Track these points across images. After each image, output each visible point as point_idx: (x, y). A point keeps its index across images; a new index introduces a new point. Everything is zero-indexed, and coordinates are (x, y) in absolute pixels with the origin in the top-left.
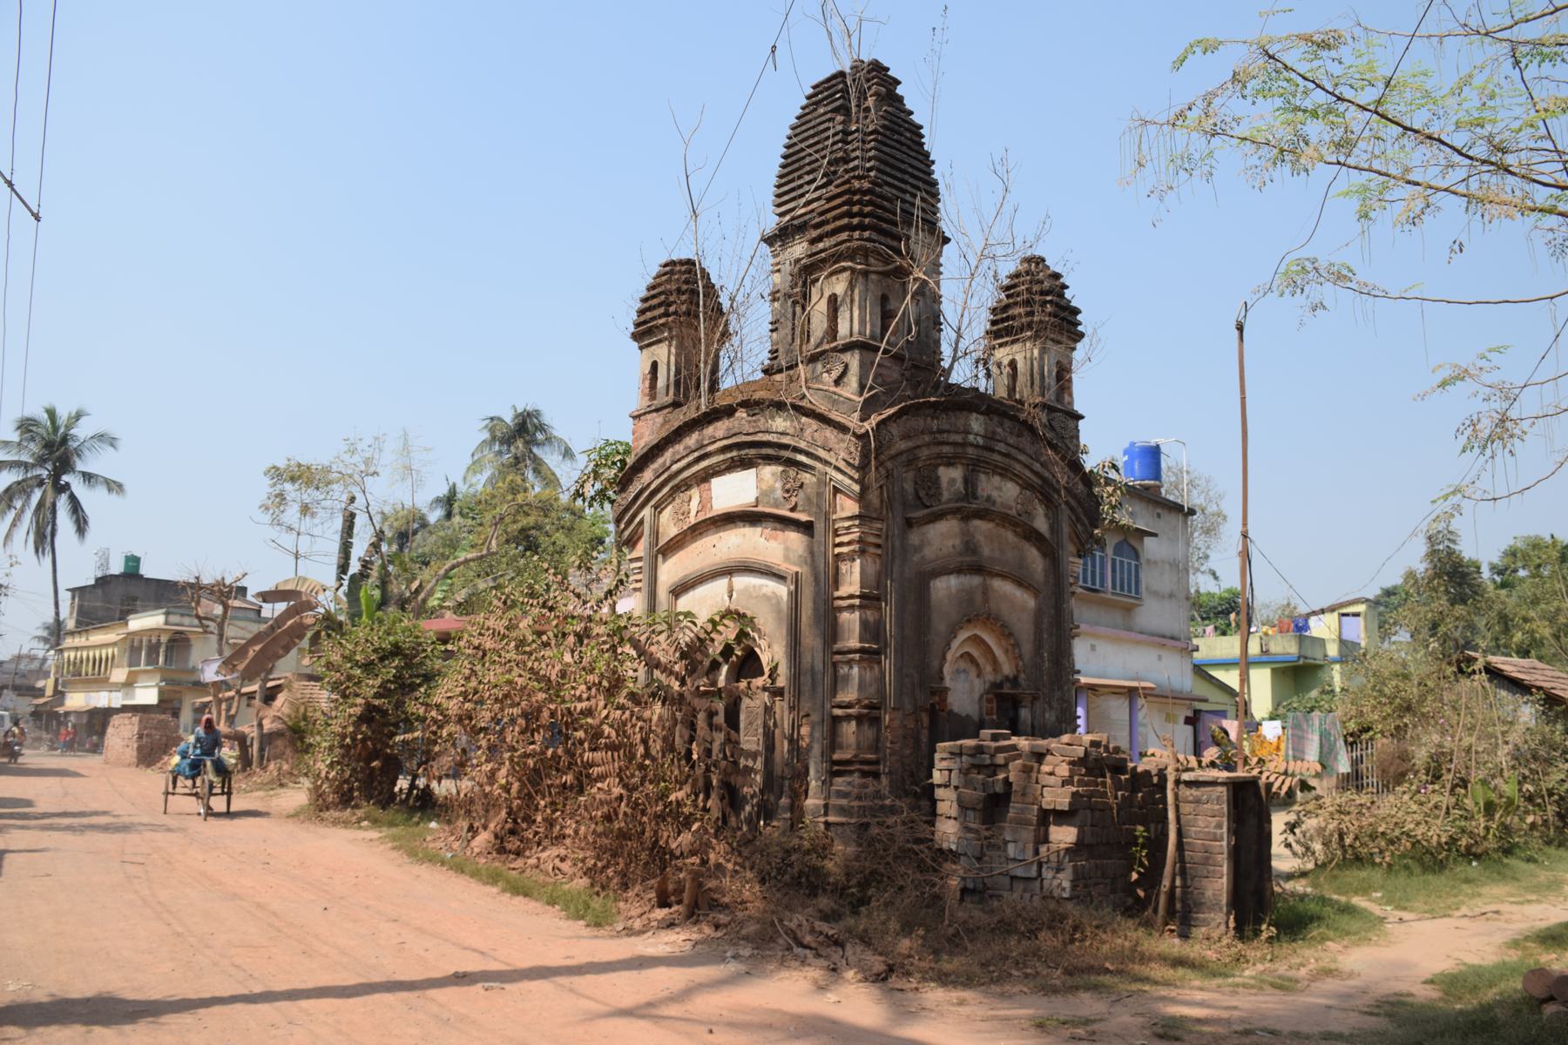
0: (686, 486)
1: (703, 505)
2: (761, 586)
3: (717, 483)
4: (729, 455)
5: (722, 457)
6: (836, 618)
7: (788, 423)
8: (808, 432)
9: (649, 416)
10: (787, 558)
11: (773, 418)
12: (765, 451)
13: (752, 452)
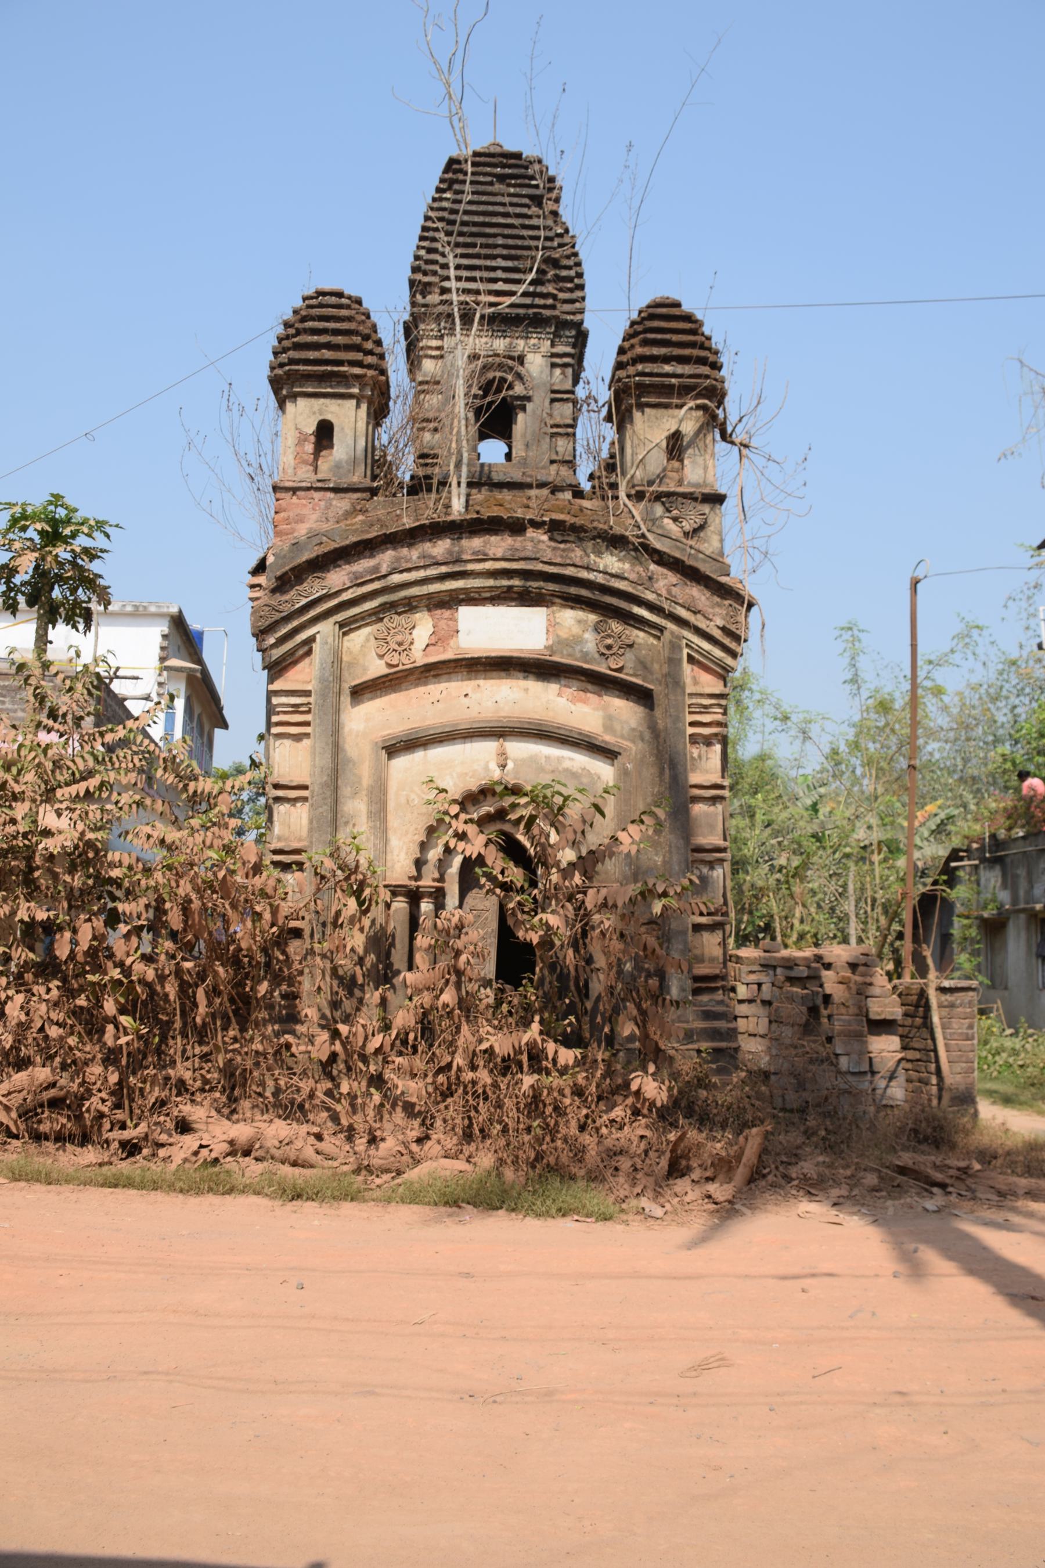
0: (410, 606)
1: (437, 640)
2: (560, 759)
3: (466, 614)
4: (505, 582)
5: (491, 582)
6: (687, 811)
7: (627, 566)
8: (661, 585)
9: (317, 495)
10: (608, 728)
11: (599, 554)
12: (573, 590)
13: (552, 587)
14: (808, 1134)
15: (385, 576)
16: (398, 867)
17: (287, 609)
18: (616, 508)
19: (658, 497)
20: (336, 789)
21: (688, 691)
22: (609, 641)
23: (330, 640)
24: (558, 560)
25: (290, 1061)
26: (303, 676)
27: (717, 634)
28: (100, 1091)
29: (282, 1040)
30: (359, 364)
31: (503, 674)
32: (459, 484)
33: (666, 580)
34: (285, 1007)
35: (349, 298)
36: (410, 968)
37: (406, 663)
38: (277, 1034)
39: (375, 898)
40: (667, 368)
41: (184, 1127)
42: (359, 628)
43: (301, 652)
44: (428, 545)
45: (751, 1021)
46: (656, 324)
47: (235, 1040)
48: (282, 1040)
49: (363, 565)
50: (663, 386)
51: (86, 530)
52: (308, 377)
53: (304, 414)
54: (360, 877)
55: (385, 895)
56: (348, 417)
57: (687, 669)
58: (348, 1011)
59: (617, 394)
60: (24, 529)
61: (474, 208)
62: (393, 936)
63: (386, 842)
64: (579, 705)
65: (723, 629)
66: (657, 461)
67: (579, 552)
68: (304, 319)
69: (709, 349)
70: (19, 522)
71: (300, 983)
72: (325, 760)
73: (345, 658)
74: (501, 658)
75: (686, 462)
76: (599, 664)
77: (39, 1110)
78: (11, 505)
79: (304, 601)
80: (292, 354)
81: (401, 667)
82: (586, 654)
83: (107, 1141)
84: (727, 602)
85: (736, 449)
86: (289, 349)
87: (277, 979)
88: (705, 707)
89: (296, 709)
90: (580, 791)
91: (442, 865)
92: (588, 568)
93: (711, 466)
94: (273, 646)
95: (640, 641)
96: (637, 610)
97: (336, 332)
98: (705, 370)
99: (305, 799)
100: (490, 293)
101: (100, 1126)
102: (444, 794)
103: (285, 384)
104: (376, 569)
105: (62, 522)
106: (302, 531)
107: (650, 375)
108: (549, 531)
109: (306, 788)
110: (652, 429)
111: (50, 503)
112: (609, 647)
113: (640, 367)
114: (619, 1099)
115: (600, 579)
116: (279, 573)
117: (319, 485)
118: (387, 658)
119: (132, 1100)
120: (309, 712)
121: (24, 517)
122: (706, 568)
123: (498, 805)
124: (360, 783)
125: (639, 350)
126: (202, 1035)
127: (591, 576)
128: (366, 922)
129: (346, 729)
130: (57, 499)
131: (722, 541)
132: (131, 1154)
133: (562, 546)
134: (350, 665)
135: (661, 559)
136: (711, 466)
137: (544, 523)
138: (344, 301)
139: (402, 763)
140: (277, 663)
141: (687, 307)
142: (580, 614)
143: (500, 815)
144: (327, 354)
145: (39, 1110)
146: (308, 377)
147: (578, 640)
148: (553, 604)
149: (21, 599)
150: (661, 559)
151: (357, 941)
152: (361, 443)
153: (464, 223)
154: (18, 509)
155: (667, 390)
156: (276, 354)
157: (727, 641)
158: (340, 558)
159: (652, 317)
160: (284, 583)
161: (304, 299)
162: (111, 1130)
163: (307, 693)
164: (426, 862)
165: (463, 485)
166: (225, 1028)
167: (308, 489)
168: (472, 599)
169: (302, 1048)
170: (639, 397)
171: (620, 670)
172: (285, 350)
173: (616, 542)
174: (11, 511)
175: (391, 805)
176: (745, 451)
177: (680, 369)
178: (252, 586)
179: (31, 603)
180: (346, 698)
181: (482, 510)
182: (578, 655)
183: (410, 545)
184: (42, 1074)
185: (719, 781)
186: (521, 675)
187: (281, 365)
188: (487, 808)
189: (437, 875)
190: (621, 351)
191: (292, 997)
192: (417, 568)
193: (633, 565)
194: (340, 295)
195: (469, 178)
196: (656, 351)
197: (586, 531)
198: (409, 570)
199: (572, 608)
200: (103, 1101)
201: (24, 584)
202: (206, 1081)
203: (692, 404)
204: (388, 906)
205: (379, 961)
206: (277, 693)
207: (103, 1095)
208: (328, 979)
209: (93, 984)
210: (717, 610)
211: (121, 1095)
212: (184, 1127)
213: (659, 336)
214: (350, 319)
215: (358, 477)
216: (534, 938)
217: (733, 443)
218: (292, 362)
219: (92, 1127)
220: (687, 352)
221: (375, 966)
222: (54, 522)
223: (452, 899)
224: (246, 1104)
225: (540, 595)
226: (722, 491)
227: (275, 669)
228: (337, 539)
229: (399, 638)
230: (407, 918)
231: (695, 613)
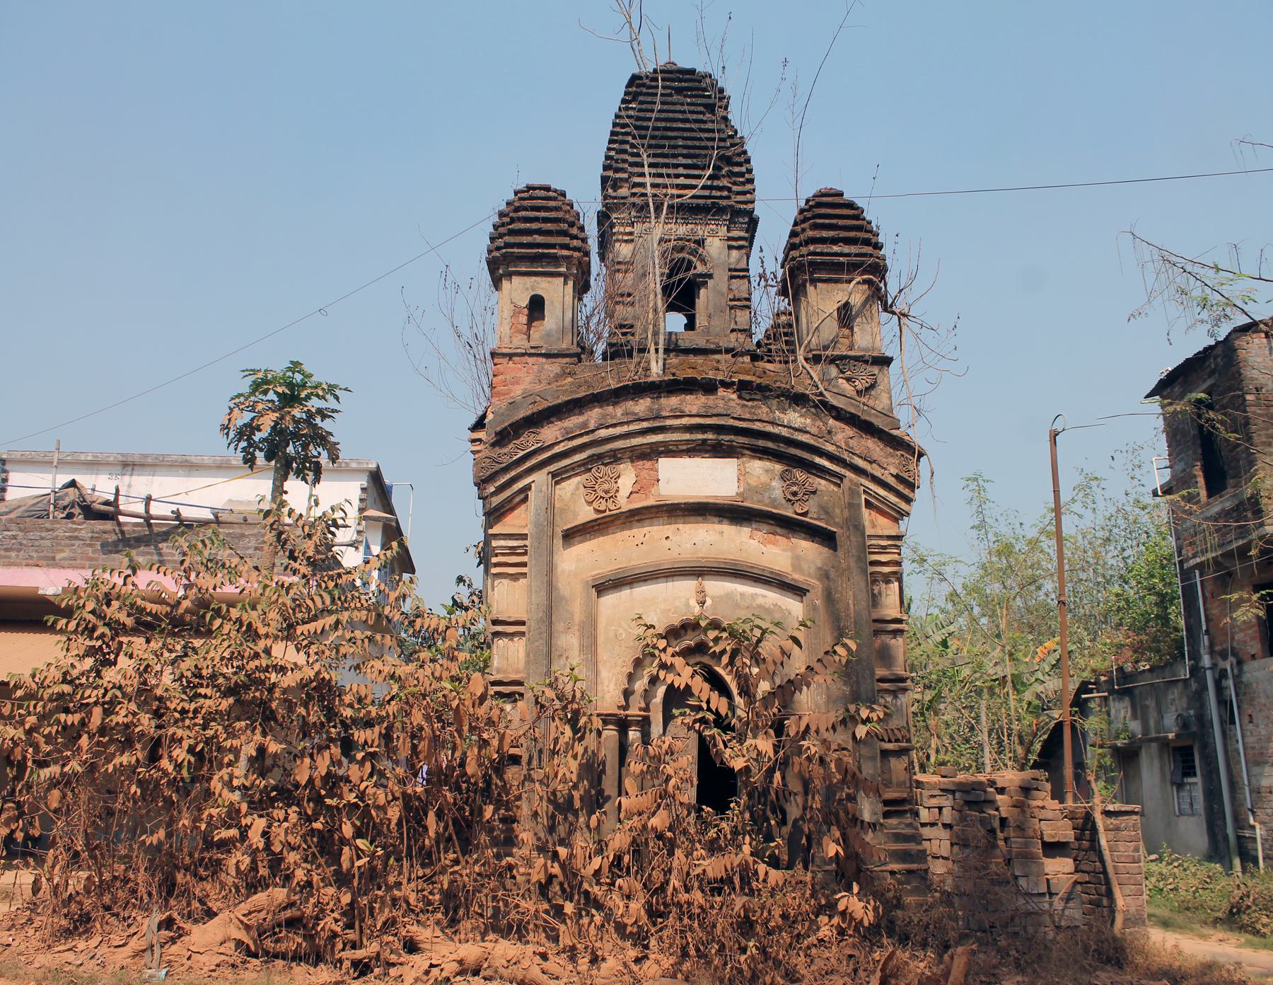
0: (615, 457)
2: (754, 596)
3: (664, 464)
4: (700, 436)
5: (687, 436)
7: (808, 421)
10: (796, 567)
11: (783, 411)
12: (761, 443)
13: (741, 440)
14: (1003, 953)
15: (593, 431)
16: (607, 696)
17: (506, 461)
18: (796, 369)
19: (832, 360)
20: (551, 624)
21: (867, 533)
22: (795, 489)
23: (544, 488)
24: (747, 416)
25: (509, 883)
26: (516, 521)
27: (892, 481)
28: (332, 911)
29: (504, 863)
30: (566, 247)
31: (700, 518)
32: (657, 350)
33: (843, 434)
34: (502, 832)
35: (555, 191)
36: (620, 795)
37: (611, 508)
38: (498, 857)
39: (589, 726)
40: (836, 249)
41: (412, 947)
42: (569, 477)
43: (517, 499)
44: (629, 405)
45: (938, 842)
46: (823, 211)
47: (456, 862)
48: (504, 863)
49: (573, 422)
50: (833, 264)
51: (321, 393)
52: (522, 258)
53: (519, 289)
54: (575, 706)
55: (597, 723)
56: (556, 292)
57: (865, 512)
58: (563, 835)
59: (791, 270)
60: (265, 392)
61: (664, 115)
62: (604, 763)
63: (597, 674)
64: (769, 546)
65: (897, 477)
66: (830, 329)
67: (765, 409)
68: (517, 210)
69: (871, 232)
70: (260, 386)
71: (518, 807)
72: (541, 598)
73: (557, 505)
74: (699, 503)
75: (855, 329)
76: (786, 509)
77: (277, 930)
78: (255, 372)
79: (521, 454)
80: (508, 239)
81: (608, 513)
82: (774, 500)
83: (341, 961)
84: (899, 453)
85: (895, 318)
86: (505, 235)
87: (499, 804)
88: (884, 547)
89: (513, 551)
90: (777, 624)
91: (647, 695)
92: (772, 423)
93: (876, 333)
94: (493, 494)
95: (822, 488)
96: (818, 460)
97: (546, 220)
98: (868, 250)
99: (523, 634)
100: (678, 187)
101: (333, 946)
102: (651, 630)
103: (500, 266)
104: (585, 424)
105: (298, 385)
106: (518, 391)
107: (821, 254)
108: (738, 390)
109: (523, 623)
110: (823, 301)
111: (289, 369)
112: (795, 494)
113: (812, 248)
114: (823, 919)
115: (785, 432)
116: (498, 429)
117: (533, 351)
118: (595, 505)
119: (362, 920)
120: (525, 553)
121: (265, 381)
122: (879, 422)
123: (697, 639)
124: (572, 619)
125: (810, 233)
126: (427, 858)
127: (776, 430)
128: (579, 749)
129: (559, 570)
130: (295, 366)
131: (890, 398)
132: (363, 974)
133: (750, 404)
134: (562, 510)
135: (839, 414)
136: (876, 333)
137: (733, 383)
138: (551, 194)
139: (610, 599)
140: (496, 509)
141: (848, 196)
142: (768, 464)
143: (701, 648)
144: (539, 239)
145: (277, 930)
146: (522, 258)
147: (767, 487)
148: (743, 455)
149: (260, 455)
150: (839, 414)
151: (574, 765)
152: (569, 315)
153: (655, 129)
154: (260, 375)
155: (838, 267)
156: (492, 239)
157: (900, 488)
158: (553, 415)
159: (819, 205)
160: (502, 438)
161: (516, 193)
162: (343, 950)
163: (523, 537)
164: (633, 693)
165: (661, 351)
166: (446, 852)
167: (523, 355)
168: (671, 451)
169: (522, 870)
170: (811, 273)
171: (805, 514)
172: (501, 236)
173: (798, 400)
174: (253, 378)
175: (601, 639)
176: (904, 320)
177: (846, 249)
178: (473, 441)
179: (268, 458)
180: (558, 541)
181: (678, 373)
182: (767, 501)
183: (615, 404)
184: (280, 894)
185: (899, 616)
186: (716, 519)
187: (498, 249)
188: (689, 641)
189: (643, 705)
190: (793, 234)
191: (509, 821)
192: (622, 424)
193: (813, 420)
194: (548, 189)
195: (660, 91)
196: (825, 234)
197: (771, 390)
198: (614, 426)
199: (760, 459)
200: (336, 921)
201: (265, 440)
202: (430, 903)
203: (859, 279)
204: (599, 733)
205: (591, 786)
206: (495, 536)
207: (336, 915)
208: (545, 804)
209: (330, 807)
210: (890, 459)
211: (352, 916)
212: (412, 947)
213: (827, 221)
214: (557, 209)
215: (566, 344)
216: (738, 764)
217: (894, 313)
218: (507, 245)
219: (325, 946)
220: (852, 234)
221: (587, 792)
222: (291, 385)
223: (656, 729)
224: (466, 925)
225: (732, 447)
226: (888, 354)
227: (494, 515)
228: (549, 398)
229: (606, 486)
230: (617, 745)
231: (871, 463)
